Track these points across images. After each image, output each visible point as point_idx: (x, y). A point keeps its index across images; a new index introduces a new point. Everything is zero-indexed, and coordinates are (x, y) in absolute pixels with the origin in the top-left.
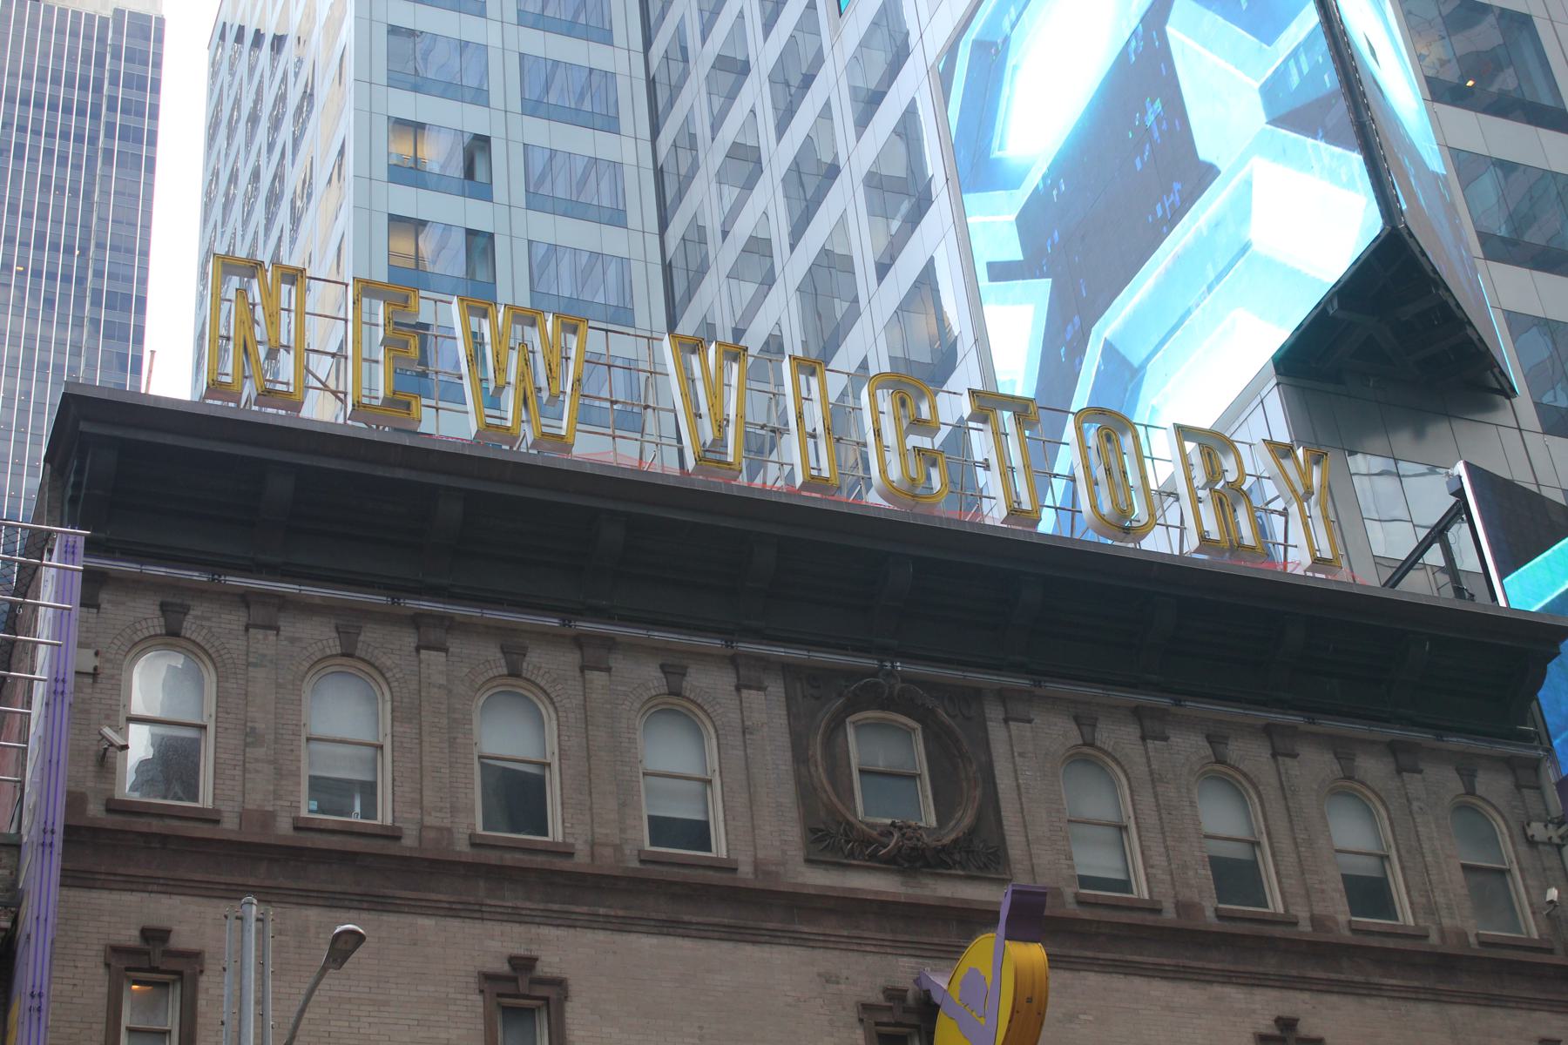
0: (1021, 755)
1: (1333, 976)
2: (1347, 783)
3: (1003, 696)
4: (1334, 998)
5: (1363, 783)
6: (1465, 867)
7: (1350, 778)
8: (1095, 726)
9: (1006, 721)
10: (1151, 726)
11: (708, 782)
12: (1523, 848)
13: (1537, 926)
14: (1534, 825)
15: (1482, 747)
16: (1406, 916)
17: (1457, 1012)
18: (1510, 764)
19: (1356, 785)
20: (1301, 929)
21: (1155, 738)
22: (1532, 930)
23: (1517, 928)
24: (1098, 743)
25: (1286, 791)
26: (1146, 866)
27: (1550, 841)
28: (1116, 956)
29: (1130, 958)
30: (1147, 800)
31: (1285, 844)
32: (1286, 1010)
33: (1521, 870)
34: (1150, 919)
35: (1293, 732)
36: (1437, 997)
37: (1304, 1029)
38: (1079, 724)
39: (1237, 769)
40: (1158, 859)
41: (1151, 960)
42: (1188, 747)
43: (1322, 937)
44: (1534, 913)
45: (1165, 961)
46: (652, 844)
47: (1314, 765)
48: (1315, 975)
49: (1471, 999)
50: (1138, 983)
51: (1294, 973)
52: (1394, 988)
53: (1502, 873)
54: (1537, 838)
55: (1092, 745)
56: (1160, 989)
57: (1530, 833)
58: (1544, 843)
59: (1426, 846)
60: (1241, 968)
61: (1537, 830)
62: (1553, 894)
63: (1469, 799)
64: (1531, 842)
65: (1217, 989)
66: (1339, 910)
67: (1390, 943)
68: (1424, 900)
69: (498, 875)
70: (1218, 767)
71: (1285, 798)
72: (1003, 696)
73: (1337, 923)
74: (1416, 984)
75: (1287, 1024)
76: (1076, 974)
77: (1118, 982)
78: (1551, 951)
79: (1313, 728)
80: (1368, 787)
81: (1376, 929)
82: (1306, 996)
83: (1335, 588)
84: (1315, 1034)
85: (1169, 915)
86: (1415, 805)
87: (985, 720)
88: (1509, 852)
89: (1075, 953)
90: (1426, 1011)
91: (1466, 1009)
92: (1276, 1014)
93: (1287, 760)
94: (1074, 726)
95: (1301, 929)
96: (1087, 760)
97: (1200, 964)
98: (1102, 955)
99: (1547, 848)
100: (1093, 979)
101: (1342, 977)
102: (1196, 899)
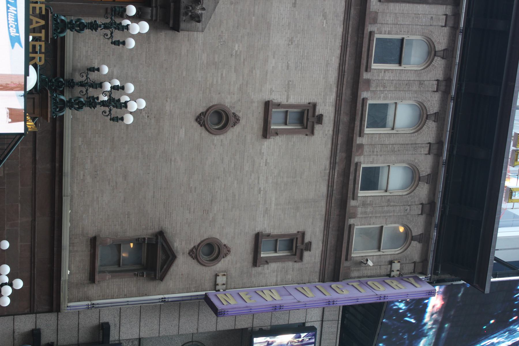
0: (432, 18)
1: (338, 151)
2: (417, 179)
3: (456, 15)
4: (329, 146)
5: (417, 186)
6: (382, 227)
7: (419, 180)
8: (443, 58)
9: (446, 15)
10: (428, 209)
11: (386, 191)
12: (389, 258)
13: (357, 257)
14: (399, 264)
15: (432, 247)
16: (361, 194)
17: (323, 204)
18: (424, 261)
19: (416, 183)
20: (358, 138)
21: (438, 85)
22: (356, 254)
23: (355, 250)
24: (436, 58)
25: (415, 146)
26: (385, 70)
27: (391, 271)
28: (349, 43)
29: (348, 49)
30: (412, 77)
31: (393, 140)
32: (325, 120)
33: (380, 255)
34: (350, 195)
35: (439, 155)
36: (329, 196)
37: (317, 127)
38: (444, 50)
39: (424, 124)
40: (387, 76)
41: (347, 59)
42: (433, 103)
43: (354, 149)
44: (362, 256)
45: (347, 66)
46: (369, 104)
47: (425, 164)
48: (339, 138)
49: (328, 213)
50: (339, 52)
51: (340, 128)
52: (333, 178)
53: (379, 249)
54: (393, 264)
55: (435, 55)
56: (335, 62)
57: (396, 261)
58: (391, 268)
59: (391, 208)
60: (343, 103)
61: (396, 266)
62: (370, 263)
63: (410, 238)
64: (391, 263)
65: (334, 90)
66: (365, 161)
67: (351, 177)
68: (369, 202)
69: (346, 174)
70: (425, 116)
71: (412, 144)
72: (456, 15)
73: (360, 155)
74: (335, 187)
75: (320, 119)
76: (342, 23)
77: (338, 43)
78: (346, 259)
79: (441, 163)
80: (415, 188)
81: (357, 175)
82: (331, 132)
83: (503, 172)
84: (316, 132)
85: (365, 76)
86: (408, 208)
87: (446, 5)
88: (389, 252)
89: (351, 23)
90: (323, 189)
91: (324, 210)
92: (324, 115)
93: (427, 149)
94: (443, 48)
95: (358, 138)
96: (429, 53)
97: (345, 83)
98: (349, 36)
99: (389, 270)
100: (340, 30)
101: (338, 155)
102: (371, 89)
